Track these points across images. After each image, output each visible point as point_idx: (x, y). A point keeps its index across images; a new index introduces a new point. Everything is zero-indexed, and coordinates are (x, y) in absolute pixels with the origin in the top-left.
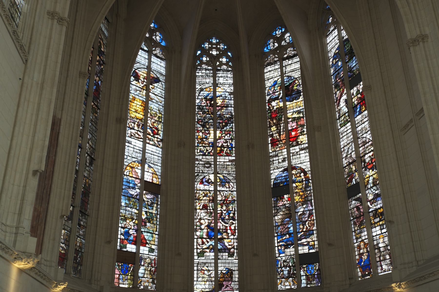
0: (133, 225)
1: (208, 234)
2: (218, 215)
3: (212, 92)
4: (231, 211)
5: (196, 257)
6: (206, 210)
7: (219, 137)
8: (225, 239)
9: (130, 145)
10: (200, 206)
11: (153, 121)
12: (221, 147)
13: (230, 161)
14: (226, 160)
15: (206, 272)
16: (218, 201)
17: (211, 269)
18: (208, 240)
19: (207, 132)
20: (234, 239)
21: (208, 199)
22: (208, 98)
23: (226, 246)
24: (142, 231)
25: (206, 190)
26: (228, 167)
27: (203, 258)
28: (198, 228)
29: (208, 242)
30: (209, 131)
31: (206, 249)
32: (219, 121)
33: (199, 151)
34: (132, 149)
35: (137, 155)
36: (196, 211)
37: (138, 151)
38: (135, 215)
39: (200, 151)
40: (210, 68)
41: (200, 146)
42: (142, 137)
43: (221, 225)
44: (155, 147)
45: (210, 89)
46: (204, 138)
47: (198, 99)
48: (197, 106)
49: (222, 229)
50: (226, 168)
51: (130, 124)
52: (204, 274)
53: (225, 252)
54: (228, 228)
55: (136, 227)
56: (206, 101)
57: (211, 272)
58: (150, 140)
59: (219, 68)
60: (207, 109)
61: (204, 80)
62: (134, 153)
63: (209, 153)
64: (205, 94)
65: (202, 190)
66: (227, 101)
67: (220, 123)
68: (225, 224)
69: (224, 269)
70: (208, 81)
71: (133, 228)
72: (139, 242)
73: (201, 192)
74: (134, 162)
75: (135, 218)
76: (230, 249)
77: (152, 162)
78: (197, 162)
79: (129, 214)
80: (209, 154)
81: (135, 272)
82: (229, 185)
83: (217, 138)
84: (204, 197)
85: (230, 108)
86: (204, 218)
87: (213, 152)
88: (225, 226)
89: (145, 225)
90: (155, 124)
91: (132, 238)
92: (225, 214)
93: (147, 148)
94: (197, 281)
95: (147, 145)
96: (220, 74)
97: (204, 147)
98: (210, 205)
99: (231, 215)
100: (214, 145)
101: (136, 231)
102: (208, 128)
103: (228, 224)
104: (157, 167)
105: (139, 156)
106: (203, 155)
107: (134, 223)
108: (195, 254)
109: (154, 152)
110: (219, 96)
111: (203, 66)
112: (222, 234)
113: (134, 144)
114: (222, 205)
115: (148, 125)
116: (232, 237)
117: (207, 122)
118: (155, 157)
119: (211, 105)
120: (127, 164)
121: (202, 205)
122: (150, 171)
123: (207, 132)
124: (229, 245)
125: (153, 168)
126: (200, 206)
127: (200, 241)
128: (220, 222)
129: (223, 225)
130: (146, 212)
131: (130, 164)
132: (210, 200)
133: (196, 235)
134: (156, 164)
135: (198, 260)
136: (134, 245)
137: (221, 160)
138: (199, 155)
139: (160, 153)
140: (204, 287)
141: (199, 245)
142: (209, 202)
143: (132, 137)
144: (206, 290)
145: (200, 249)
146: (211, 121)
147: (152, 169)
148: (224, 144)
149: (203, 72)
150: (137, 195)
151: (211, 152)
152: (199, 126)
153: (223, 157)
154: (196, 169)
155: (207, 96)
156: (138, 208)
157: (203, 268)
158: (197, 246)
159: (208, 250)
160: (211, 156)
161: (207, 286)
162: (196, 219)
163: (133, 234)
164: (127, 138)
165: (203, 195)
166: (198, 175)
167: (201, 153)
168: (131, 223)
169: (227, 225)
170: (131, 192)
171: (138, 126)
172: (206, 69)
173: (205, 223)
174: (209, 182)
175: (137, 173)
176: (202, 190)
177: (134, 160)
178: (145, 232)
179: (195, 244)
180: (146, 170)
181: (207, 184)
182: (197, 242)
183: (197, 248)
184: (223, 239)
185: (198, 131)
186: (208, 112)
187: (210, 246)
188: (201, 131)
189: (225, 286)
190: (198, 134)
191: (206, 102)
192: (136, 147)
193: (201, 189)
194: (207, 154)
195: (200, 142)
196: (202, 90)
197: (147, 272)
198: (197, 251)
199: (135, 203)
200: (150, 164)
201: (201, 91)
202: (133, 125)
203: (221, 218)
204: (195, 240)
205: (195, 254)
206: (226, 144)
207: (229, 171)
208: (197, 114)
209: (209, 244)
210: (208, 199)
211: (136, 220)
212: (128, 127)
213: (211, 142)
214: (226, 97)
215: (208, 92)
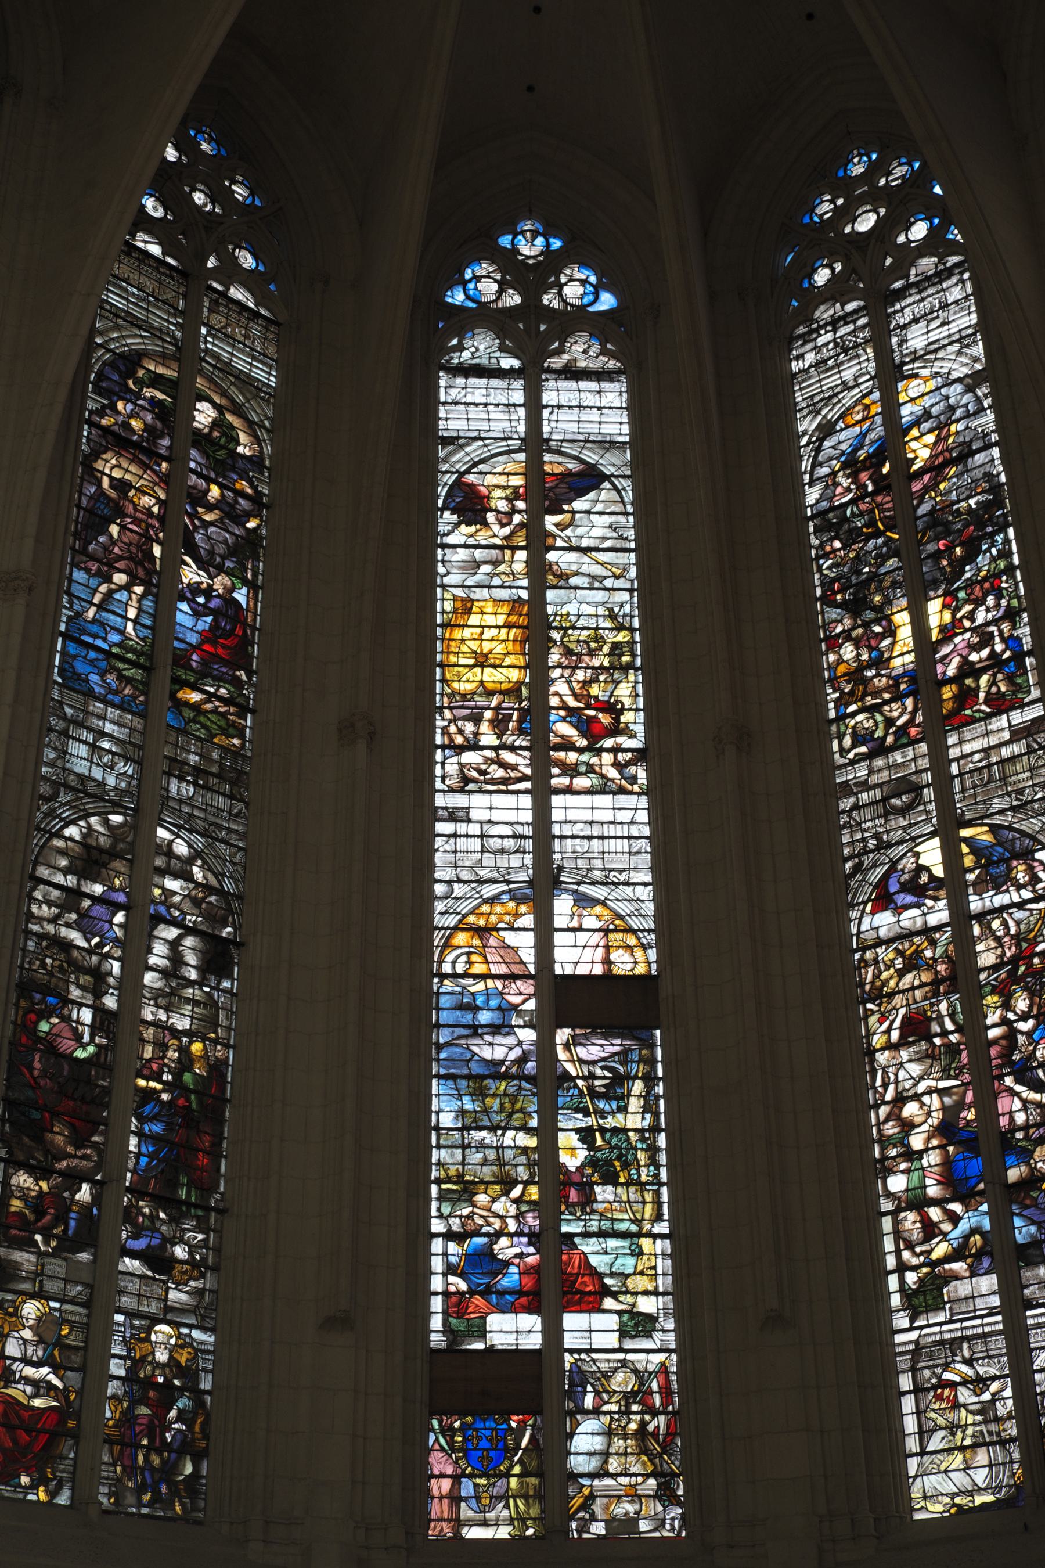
0: (513, 1210)
1: (949, 1175)
2: (994, 1051)
3: (879, 420)
5: (902, 1321)
6: (924, 1045)
7: (942, 628)
9: (462, 828)
11: (580, 675)
13: (1017, 734)
14: (994, 740)
15: (965, 1395)
16: (983, 976)
18: (956, 1207)
19: (878, 629)
21: (926, 977)
22: (862, 454)
24: (570, 1236)
26: (1010, 769)
27: (941, 1317)
28: (893, 1152)
30: (888, 618)
32: (931, 548)
33: (847, 741)
34: (476, 844)
35: (502, 862)
37: (509, 843)
38: (523, 1159)
40: (850, 307)
42: (528, 771)
44: (606, 800)
45: (867, 407)
46: (869, 667)
47: (811, 484)
48: (813, 517)
50: (1004, 778)
51: (453, 729)
52: (956, 1405)
55: (532, 1221)
56: (854, 476)
58: (571, 770)
59: (898, 285)
60: (861, 514)
61: (834, 380)
62: (488, 860)
63: (903, 730)
64: (844, 447)
65: (888, 942)
67: (937, 555)
70: (848, 375)
71: (512, 1226)
72: (550, 1293)
73: (885, 954)
74: (493, 900)
75: (523, 1173)
77: (597, 874)
78: (846, 803)
79: (485, 1162)
80: (904, 738)
81: (552, 1448)
83: (935, 635)
84: (901, 974)
86: (921, 1088)
87: (919, 718)
89: (588, 1200)
90: (595, 690)
91: (511, 1279)
93: (556, 815)
94: (923, 1453)
95: (556, 800)
96: (907, 310)
97: (871, 710)
98: (943, 1007)
100: (921, 682)
101: (534, 1238)
102: (879, 609)
104: (629, 890)
105: (521, 866)
106: (870, 756)
107: (517, 1201)
108: (896, 1300)
109: (608, 822)
110: (917, 423)
111: (817, 314)
113: (484, 815)
115: (554, 701)
117: (873, 577)
118: (611, 845)
119: (883, 485)
120: (451, 921)
121: (897, 1024)
122: (590, 922)
123: (878, 629)
125: (603, 903)
127: (910, 1220)
130: (586, 1135)
131: (471, 919)
133: (889, 1195)
134: (622, 878)
135: (914, 1335)
136: (530, 1311)
137: (968, 748)
138: (853, 762)
139: (643, 816)
141: (910, 1246)
143: (471, 786)
145: (915, 1268)
146: (892, 563)
147: (598, 909)
148: (974, 657)
149: (820, 341)
150: (522, 1060)
151: (911, 722)
152: (833, 614)
153: (980, 727)
154: (846, 839)
155: (856, 450)
156: (534, 1123)
157: (947, 1376)
158: (898, 1252)
159: (959, 1267)
160: (913, 742)
161: (980, 1476)
163: (520, 1256)
164: (440, 800)
165: (899, 963)
166: (857, 868)
167: (863, 749)
168: (497, 1207)
170: (487, 1053)
171: (499, 725)
172: (834, 323)
173: (924, 1114)
174: (919, 887)
175: (515, 950)
176: (888, 942)
177: (489, 891)
178: (586, 1235)
180: (559, 922)
183: (902, 1268)
185: (834, 643)
186: (872, 523)
188: (847, 636)
190: (832, 658)
192: (495, 830)
193: (883, 933)
194: (890, 739)
195: (852, 693)
196: (827, 430)
197: (619, 1444)
198: (902, 1281)
199: (514, 1098)
200: (582, 888)
201: (821, 440)
202: (469, 727)
204: (887, 1224)
205: (896, 1300)
206: (985, 653)
207: (1020, 792)
208: (818, 557)
209: (964, 1226)
210: (926, 977)
211: (526, 1184)
212: (443, 747)
213: (905, 674)
215: (857, 430)
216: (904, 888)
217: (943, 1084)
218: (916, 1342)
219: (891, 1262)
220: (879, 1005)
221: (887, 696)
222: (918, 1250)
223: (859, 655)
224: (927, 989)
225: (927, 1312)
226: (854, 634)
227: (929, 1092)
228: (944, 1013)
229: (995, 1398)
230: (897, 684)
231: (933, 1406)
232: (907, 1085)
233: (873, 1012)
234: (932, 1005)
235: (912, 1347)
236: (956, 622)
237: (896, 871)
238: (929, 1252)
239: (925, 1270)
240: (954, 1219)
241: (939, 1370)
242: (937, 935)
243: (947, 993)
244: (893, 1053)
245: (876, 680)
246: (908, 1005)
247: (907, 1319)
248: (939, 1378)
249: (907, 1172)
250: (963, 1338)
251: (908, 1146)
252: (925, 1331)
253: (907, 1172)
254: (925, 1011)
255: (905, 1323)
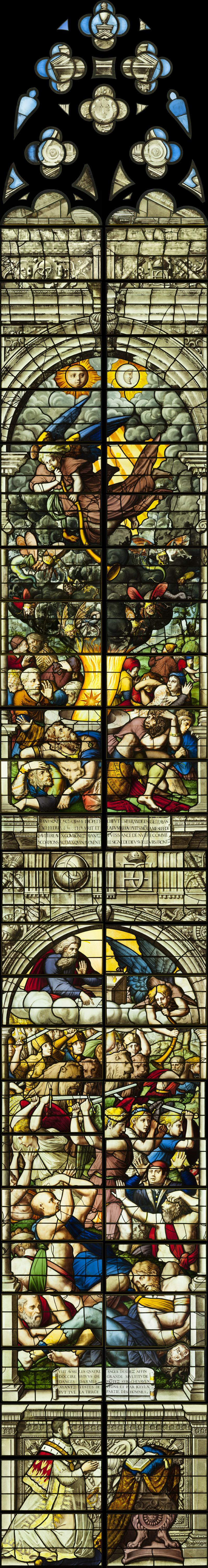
1: (70, 1271)
4: (174, 1137)
5: (11, 1395)
6: (62, 1140)
8: (144, 1293)
10: (29, 1115)
12: (129, 761)
15: (58, 1467)
17: (87, 1451)
18: (74, 1300)
20: (188, 1293)
23: (145, 1333)
25: (62, 1024)
27: (45, 1396)
28: (21, 1236)
29: (71, 1311)
31: (60, 1346)
36: (9, 1143)
39: (30, 790)
41: (29, 760)
43: (125, 1220)
49: (130, 1242)
52: (49, 1475)
53: (140, 1364)
54: (161, 1234)
57: (87, 1466)
63: (78, 797)
66: (170, 451)
68: (142, 1215)
69: (139, 1451)
76: (168, 1345)
82: (169, 993)
84: (49, 1061)
85: (185, 502)
86: (53, 1181)
88: (143, 1223)
92: (144, 1155)
94: (17, 1511)
98: (85, 1106)
99: (178, 1161)
103: (159, 1210)
108: (7, 1375)
112: (126, 1268)
114: (126, 1105)
116: (181, 1283)
121: (38, 1111)
124: (163, 1327)
126: (29, 1115)
127: (28, 1302)
128: (119, 1202)
129: (131, 1216)
132: (80, 1079)
133: (11, 1275)
135: (20, 1409)
140: (47, 1537)
141: (27, 1327)
142: (79, 1091)
144: (61, 1556)
157: (47, 1448)
159: (70, 1356)
161: (66, 1537)
162: (9, 1188)
165: (47, 1051)
166: (17, 935)
167: (34, 802)
169: (152, 1218)
179: (7, 1320)
181: (65, 987)
182: (15, 1312)
183: (17, 1346)
184: (129, 1292)
187: (80, 1330)
189: (140, 1534)
191: (61, 466)
193: (35, 1014)
194: (64, 801)
198: (15, 1360)
203: (125, 1178)
204: (7, 1301)
205: (7, 1375)
206: (159, 741)
209: (78, 1320)
210: (71, 1071)
213: (87, 733)
214: (165, 424)
216: (61, 973)
217: (74, 1182)
218: (22, 1415)
219: (7, 1340)
220: (23, 1088)
221: (67, 751)
222: (34, 1332)
223: (41, 688)
224: (71, 1084)
225: (35, 1390)
226: (40, 659)
227: (63, 1186)
228: (85, 1113)
229: (86, 1475)
230: (79, 742)
231: (30, 1473)
232: (42, 1174)
233: (16, 1094)
234: (74, 1102)
235: (18, 1418)
236: (133, 692)
237: (54, 952)
238: (44, 1336)
239: (39, 1352)
240: (71, 1311)
241: (39, 1443)
242: (88, 1033)
243: (89, 1094)
244: (31, 1140)
245: (57, 728)
246: (50, 1095)
247: (16, 1394)
248: (40, 1451)
249: (32, 1258)
250: (64, 1419)
251: (35, 1233)
252: (31, 1407)
253: (32, 1258)
254: (67, 1107)
255: (14, 1397)
